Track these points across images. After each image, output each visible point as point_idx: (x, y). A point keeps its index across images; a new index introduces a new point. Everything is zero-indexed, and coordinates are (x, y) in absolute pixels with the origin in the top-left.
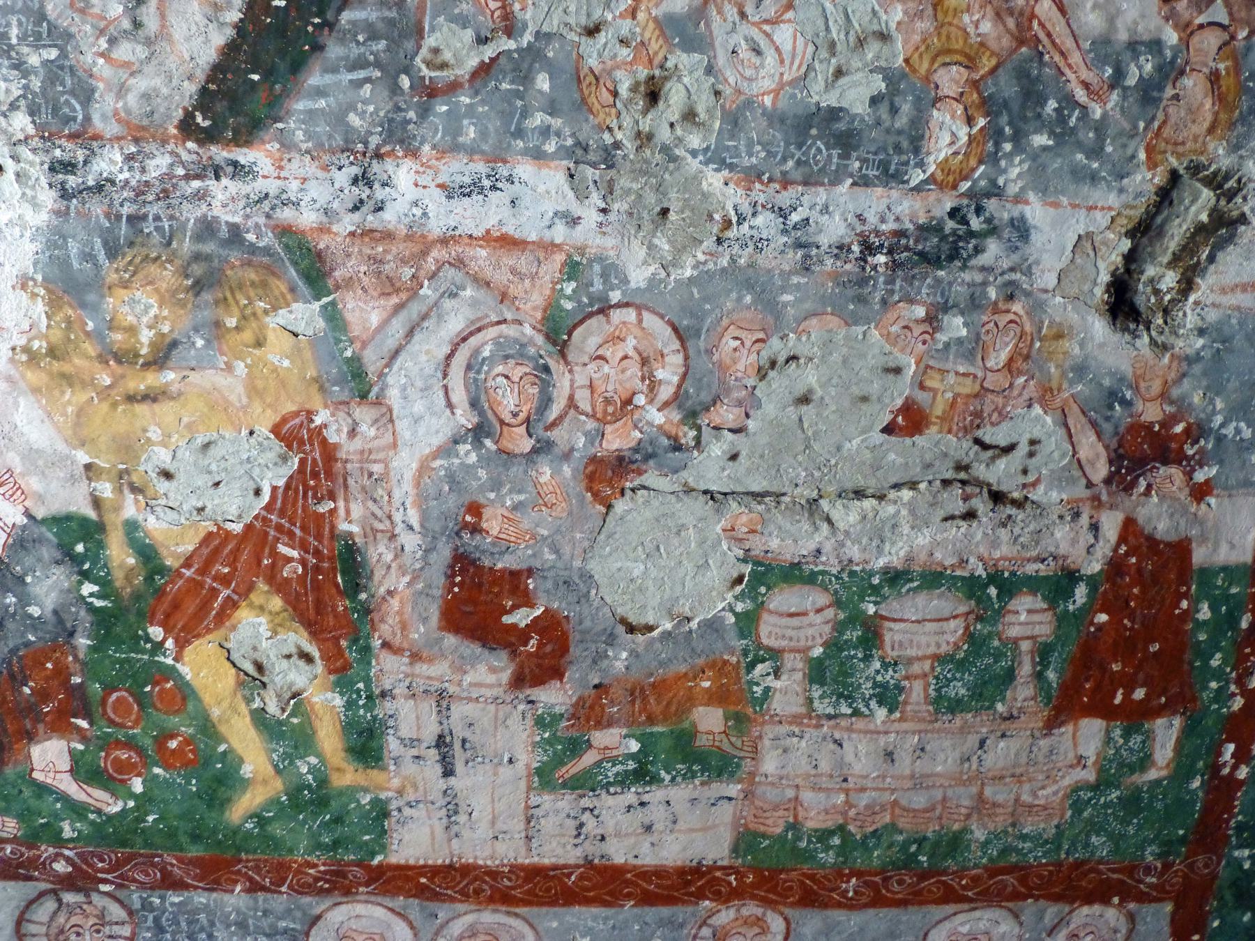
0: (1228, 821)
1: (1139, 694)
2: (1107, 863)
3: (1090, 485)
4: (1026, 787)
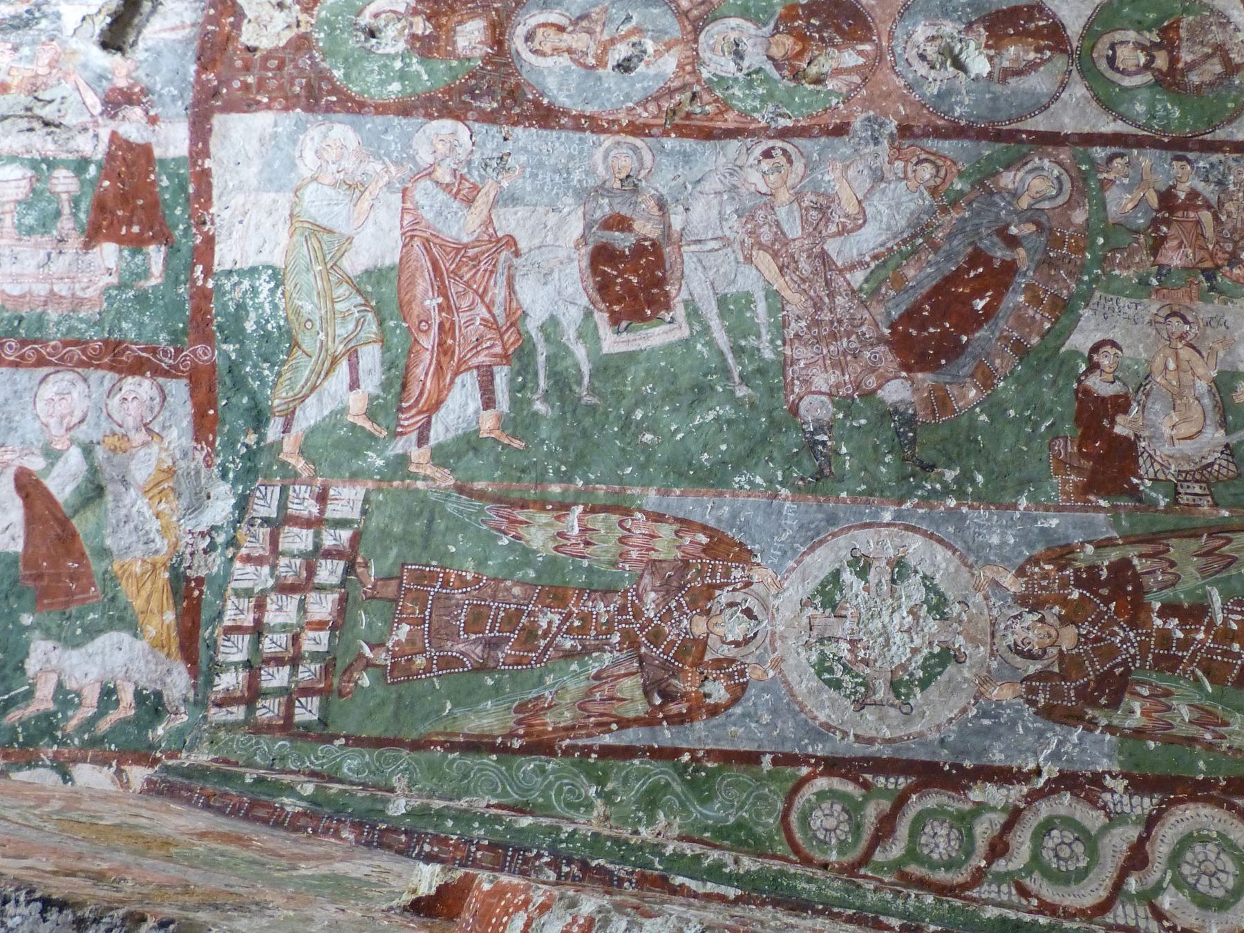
0: (211, 321)
1: (136, 229)
2: (136, 344)
3: (92, 116)
4: (77, 286)
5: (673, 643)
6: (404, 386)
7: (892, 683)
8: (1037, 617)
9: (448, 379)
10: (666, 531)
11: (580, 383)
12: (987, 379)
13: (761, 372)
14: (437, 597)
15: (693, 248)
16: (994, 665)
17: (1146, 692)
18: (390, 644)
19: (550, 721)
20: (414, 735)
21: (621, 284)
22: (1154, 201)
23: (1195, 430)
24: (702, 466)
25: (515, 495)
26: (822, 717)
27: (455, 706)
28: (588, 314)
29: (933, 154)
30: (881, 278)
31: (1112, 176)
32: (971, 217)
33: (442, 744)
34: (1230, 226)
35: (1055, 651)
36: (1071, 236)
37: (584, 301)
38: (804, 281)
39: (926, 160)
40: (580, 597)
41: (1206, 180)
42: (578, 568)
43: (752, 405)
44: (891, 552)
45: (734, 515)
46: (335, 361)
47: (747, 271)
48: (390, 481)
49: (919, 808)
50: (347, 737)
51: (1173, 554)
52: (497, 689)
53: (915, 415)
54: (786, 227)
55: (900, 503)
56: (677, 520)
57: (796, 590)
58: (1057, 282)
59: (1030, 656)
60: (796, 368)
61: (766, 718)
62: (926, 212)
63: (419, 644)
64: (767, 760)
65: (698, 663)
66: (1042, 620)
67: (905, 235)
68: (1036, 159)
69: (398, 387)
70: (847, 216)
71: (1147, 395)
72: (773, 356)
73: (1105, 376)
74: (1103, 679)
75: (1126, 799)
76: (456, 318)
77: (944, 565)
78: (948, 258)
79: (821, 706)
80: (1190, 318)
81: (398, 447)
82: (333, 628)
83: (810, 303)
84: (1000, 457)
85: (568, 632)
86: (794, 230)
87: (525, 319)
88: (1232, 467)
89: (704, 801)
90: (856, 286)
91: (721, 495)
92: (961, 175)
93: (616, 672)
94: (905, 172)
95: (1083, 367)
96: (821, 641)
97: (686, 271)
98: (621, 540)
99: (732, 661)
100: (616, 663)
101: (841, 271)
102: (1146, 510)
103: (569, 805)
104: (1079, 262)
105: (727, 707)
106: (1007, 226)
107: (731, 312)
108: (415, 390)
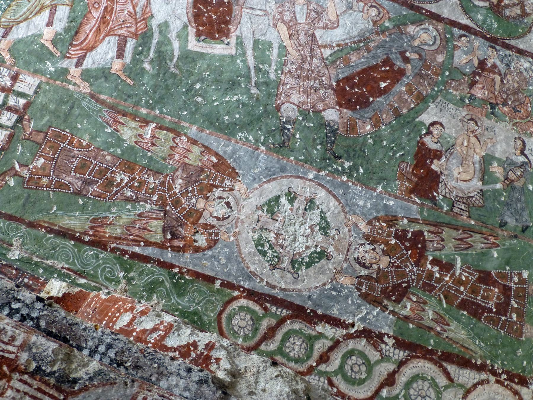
5: (185, 209)
6: (77, 33)
7: (292, 261)
8: (372, 247)
9: (101, 37)
10: (196, 150)
11: (171, 60)
12: (377, 123)
13: (267, 84)
14: (64, 149)
15: (249, 11)
16: (345, 265)
18: (31, 167)
20: (31, 219)
21: (207, 17)
22: (476, 63)
23: (468, 178)
24: (223, 122)
25: (122, 108)
26: (252, 268)
27: (58, 210)
28: (185, 27)
29: (379, 5)
30: (339, 56)
31: (460, 44)
32: (389, 41)
33: (45, 228)
34: (507, 86)
36: (434, 67)
37: (185, 19)
38: (300, 45)
39: (375, 7)
40: (141, 171)
41: (502, 61)
42: (144, 156)
43: (258, 99)
44: (308, 194)
45: (234, 152)
46: (42, 8)
47: (273, 31)
48: (55, 80)
49: (290, 328)
51: (444, 235)
52: (84, 207)
53: (337, 129)
54: (298, 16)
55: (320, 170)
56: (203, 146)
57: (255, 200)
58: (422, 86)
59: (363, 266)
60: (285, 87)
61: (223, 261)
62: (369, 32)
63: (47, 171)
64: (218, 283)
66: (374, 250)
67: (356, 39)
68: (427, 24)
69: (73, 33)
70: (330, 21)
71: (451, 154)
72: (274, 78)
73: (433, 139)
74: (396, 287)
76: (115, 7)
77: (333, 208)
78: (373, 57)
79: (254, 263)
80: (479, 124)
81: (65, 64)
83: (300, 57)
84: (374, 163)
85: (131, 187)
86: (302, 19)
87: (151, 19)
88: (481, 201)
89: (180, 295)
90: (325, 57)
91: (229, 140)
92: (390, 19)
93: (151, 215)
94: (363, 9)
95: (424, 131)
96: (262, 229)
97: (242, 21)
98: (172, 148)
99: (213, 227)
100: (151, 211)
101: (319, 46)
102: (437, 210)
103: (107, 279)
104: (435, 80)
105: (204, 250)
106: (405, 51)
107: (260, 49)
108: (82, 37)
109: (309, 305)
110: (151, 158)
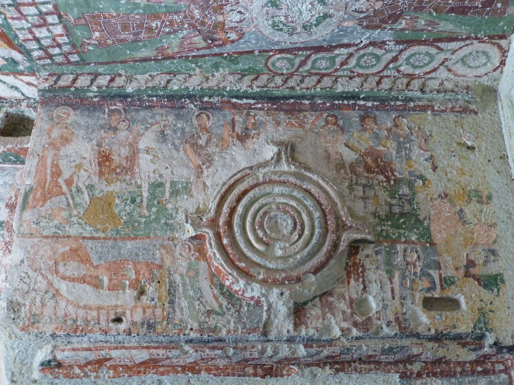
7: (303, 27)
14: (104, 23)
16: (346, 16)
17: (408, 17)
19: (170, 52)
20: (119, 60)
33: (132, 61)
35: (372, 9)
40: (165, 16)
49: (315, 57)
50: (95, 63)
52: (145, 46)
59: (362, 12)
61: (254, 42)
63: (106, 37)
64: (257, 53)
65: (223, 29)
75: (394, 46)
79: (276, 36)
82: (67, 36)
85: (166, 26)
89: (235, 64)
93: (190, 35)
96: (273, 17)
99: (237, 27)
100: (189, 33)
103: (186, 70)
105: (238, 40)
109: (325, 44)
110: (166, 6)
